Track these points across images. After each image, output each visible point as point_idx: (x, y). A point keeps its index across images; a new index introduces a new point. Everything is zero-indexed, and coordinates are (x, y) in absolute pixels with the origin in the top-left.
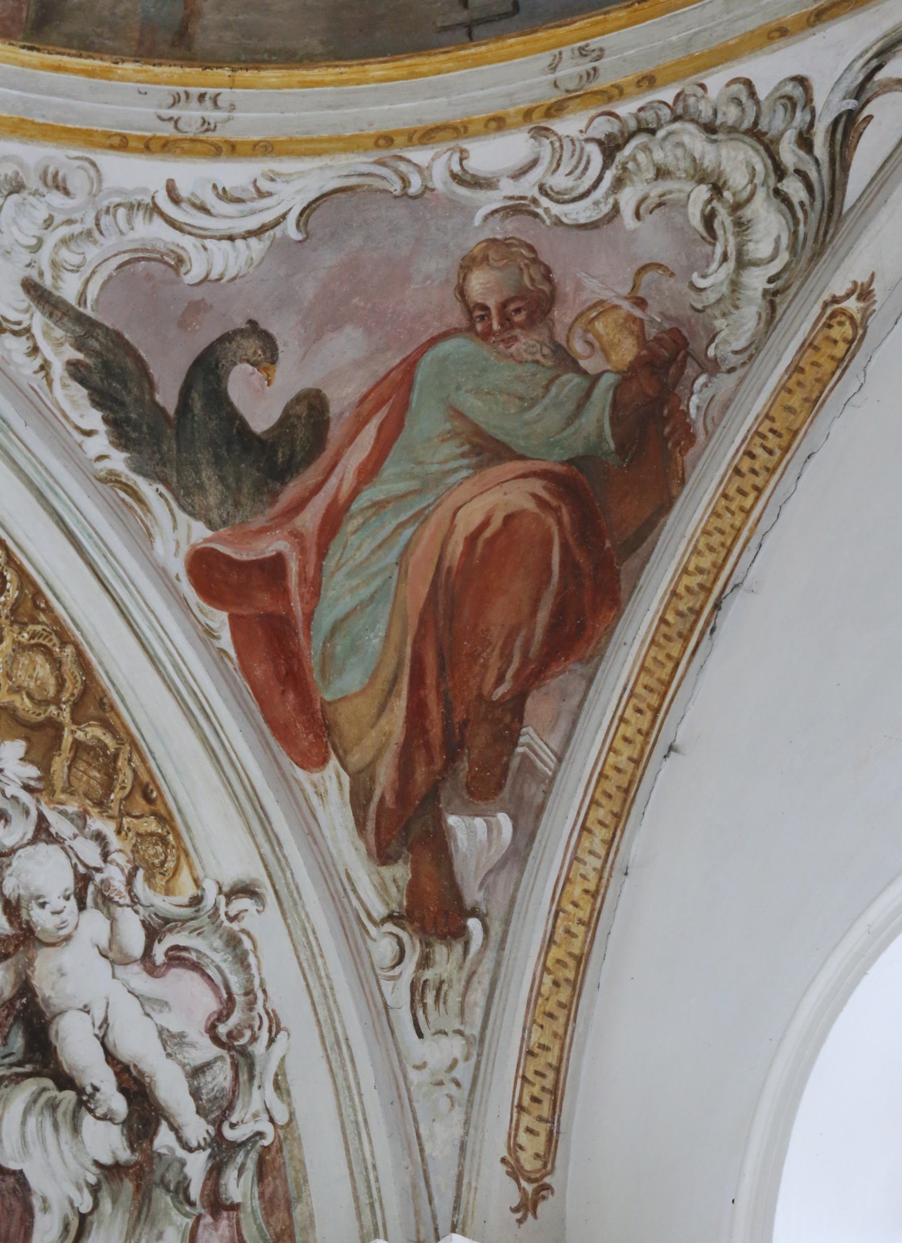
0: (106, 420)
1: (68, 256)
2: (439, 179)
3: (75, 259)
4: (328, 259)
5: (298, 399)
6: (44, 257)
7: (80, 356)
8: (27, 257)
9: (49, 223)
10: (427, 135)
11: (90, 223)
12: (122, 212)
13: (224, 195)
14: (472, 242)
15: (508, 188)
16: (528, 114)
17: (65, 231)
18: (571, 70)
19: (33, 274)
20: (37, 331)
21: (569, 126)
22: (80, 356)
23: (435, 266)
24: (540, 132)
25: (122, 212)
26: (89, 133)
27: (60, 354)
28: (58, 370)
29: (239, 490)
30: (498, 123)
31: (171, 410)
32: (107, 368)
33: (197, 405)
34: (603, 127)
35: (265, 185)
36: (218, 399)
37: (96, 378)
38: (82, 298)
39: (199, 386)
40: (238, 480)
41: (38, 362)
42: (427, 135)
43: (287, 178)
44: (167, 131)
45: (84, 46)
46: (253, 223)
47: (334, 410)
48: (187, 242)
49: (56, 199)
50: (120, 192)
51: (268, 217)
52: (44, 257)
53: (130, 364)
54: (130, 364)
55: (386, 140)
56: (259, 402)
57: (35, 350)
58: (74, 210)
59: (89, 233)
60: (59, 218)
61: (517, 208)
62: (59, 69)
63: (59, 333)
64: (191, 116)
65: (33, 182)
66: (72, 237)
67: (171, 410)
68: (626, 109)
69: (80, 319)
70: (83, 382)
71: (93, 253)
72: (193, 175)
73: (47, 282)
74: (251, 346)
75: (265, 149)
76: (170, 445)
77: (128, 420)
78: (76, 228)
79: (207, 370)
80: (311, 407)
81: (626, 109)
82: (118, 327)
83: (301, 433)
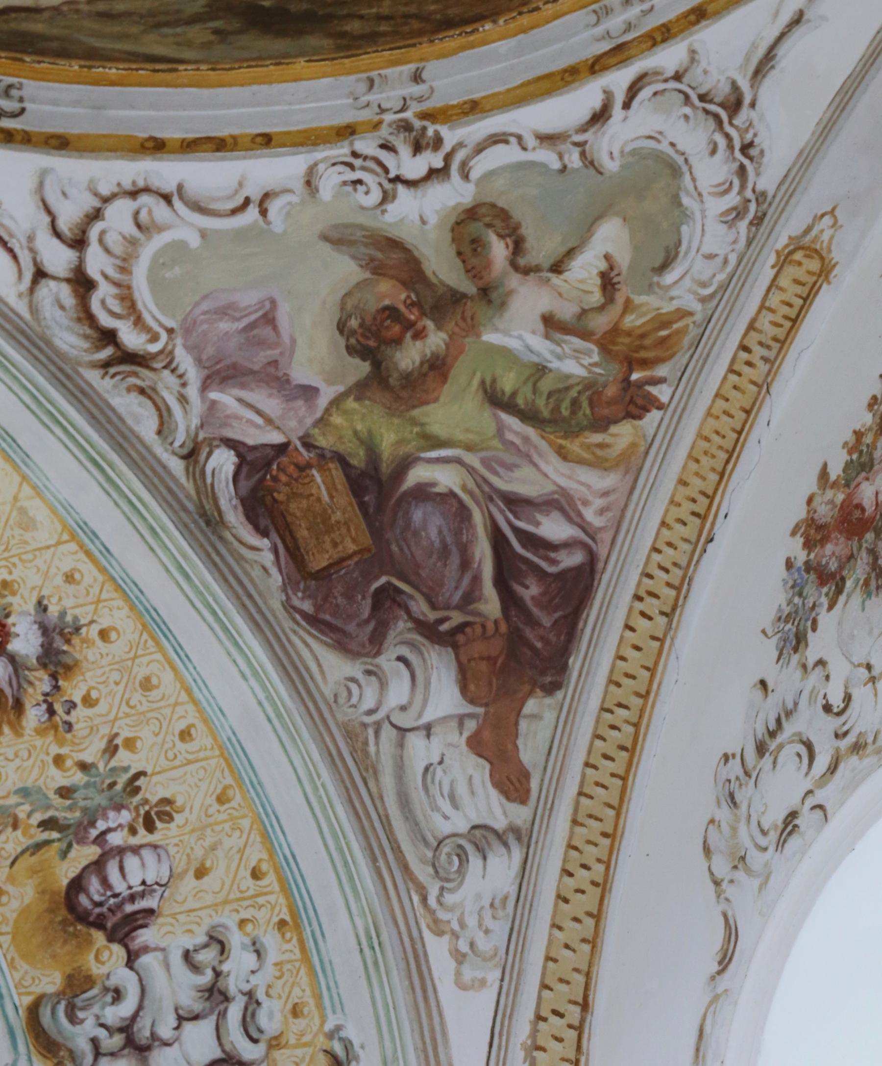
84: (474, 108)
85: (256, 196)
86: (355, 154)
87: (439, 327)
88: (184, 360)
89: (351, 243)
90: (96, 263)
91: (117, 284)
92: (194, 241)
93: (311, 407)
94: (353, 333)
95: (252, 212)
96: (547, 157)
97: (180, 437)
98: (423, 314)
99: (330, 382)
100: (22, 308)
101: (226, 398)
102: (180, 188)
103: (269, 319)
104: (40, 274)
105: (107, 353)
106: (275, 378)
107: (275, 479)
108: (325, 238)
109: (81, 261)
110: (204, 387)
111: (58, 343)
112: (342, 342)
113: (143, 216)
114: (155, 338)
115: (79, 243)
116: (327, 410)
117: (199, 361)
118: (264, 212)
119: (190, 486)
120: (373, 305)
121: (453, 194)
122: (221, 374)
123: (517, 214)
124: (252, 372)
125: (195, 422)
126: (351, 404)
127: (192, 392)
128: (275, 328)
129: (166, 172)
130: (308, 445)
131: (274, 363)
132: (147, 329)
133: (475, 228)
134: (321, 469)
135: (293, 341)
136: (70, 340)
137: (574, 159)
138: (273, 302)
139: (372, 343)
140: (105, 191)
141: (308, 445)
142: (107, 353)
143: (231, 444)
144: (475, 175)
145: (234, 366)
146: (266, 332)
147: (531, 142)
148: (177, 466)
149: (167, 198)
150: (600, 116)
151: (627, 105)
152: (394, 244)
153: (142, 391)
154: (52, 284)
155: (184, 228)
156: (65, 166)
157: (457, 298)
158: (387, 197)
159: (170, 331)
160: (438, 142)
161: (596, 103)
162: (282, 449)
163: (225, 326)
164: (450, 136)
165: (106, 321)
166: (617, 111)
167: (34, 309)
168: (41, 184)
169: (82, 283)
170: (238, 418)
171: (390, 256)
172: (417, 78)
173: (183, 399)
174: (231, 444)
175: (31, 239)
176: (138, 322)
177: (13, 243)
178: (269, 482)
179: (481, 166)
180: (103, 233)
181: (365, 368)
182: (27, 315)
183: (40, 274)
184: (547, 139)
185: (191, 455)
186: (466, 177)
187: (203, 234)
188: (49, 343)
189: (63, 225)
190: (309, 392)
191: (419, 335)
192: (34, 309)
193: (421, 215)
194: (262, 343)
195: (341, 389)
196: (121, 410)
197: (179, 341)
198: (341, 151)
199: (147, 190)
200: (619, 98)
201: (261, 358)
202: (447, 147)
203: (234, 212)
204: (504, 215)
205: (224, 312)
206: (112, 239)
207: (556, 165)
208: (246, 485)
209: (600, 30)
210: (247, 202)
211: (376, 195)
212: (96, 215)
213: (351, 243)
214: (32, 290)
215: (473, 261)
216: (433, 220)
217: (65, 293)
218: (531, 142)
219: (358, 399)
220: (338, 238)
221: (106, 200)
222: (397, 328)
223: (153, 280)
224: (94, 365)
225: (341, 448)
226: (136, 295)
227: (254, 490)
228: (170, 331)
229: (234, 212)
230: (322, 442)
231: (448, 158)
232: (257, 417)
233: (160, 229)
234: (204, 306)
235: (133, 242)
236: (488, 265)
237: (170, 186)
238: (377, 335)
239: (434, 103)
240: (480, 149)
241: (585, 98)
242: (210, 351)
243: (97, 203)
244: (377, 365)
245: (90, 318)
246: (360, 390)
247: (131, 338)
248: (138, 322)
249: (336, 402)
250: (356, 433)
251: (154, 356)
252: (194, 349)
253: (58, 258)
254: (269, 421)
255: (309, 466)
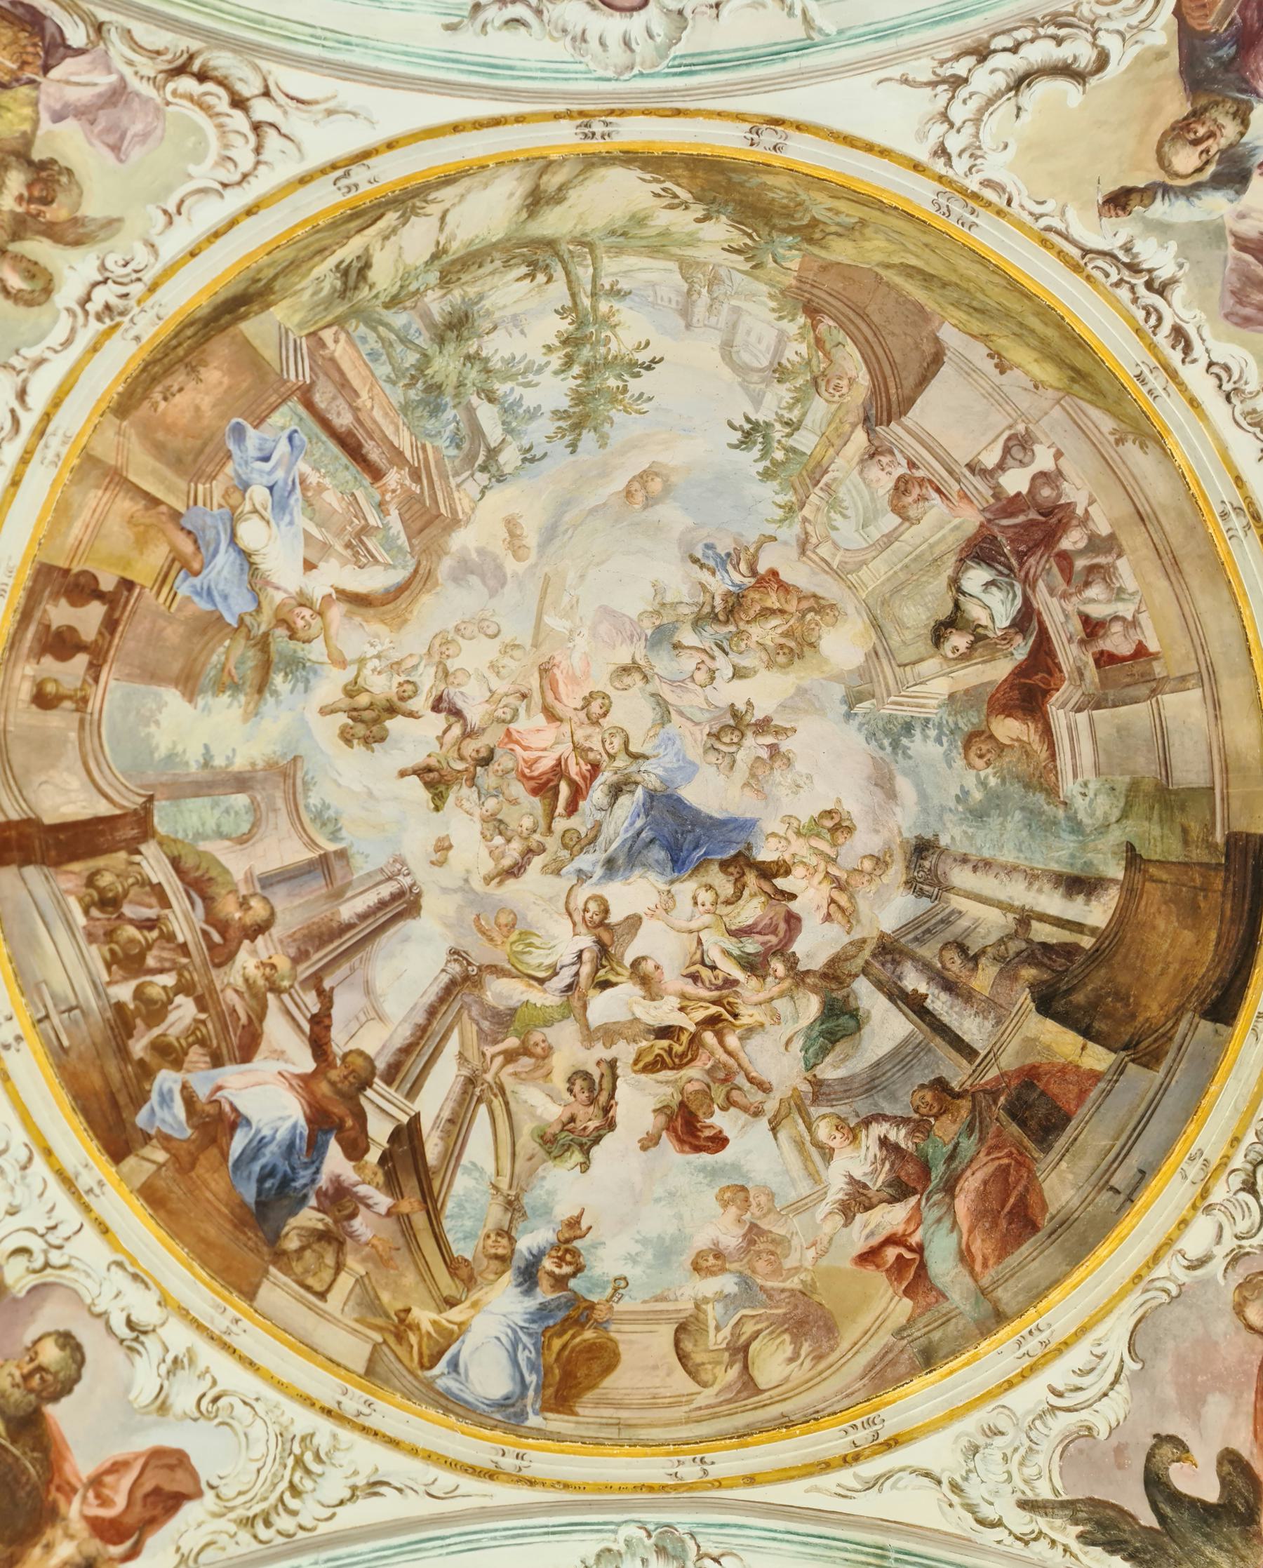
0: (1125, 1559)
1: (1030, 1471)
2: (1184, 1276)
3: (1035, 1471)
4: (1164, 1367)
5: (1220, 1464)
6: (1018, 1481)
7: (1080, 1528)
8: (1009, 1488)
9: (1006, 1459)
10: (1156, 1258)
11: (1027, 1443)
12: (1038, 1423)
13: (1083, 1373)
14: (1230, 1296)
15: (1220, 1252)
16: (1194, 1207)
17: (1017, 1457)
18: (1194, 1171)
19: (1019, 1495)
20: (1046, 1530)
21: (1219, 1193)
22: (1080, 1528)
23: (1224, 1325)
24: (1209, 1209)
25: (1038, 1423)
26: (989, 1392)
27: (1069, 1534)
28: (1075, 1546)
29: (1236, 1548)
30: (1184, 1223)
31: (1156, 1525)
32: (1100, 1524)
33: (1168, 1510)
34: (1237, 1181)
35: (1098, 1351)
36: (1177, 1499)
37: (1099, 1535)
38: (1056, 1492)
39: (1159, 1498)
40: (1230, 1541)
41: (1061, 1548)
42: (1156, 1258)
43: (1106, 1337)
44: (1027, 1362)
45: (954, 1353)
46: (1110, 1377)
47: (1245, 1454)
48: (1084, 1415)
49: (999, 1441)
50: (1028, 1412)
51: (1114, 1368)
52: (1018, 1481)
53: (1111, 1513)
54: (1111, 1513)
55: (1138, 1277)
56: (1200, 1482)
57: (1053, 1542)
58: (1013, 1441)
59: (1031, 1449)
60: (1009, 1452)
61: (1236, 1259)
62: (951, 1373)
63: (1058, 1522)
64: (1032, 1345)
65: (981, 1440)
66: (1024, 1458)
67: (1156, 1525)
68: (1238, 1161)
69: (1064, 1505)
70: (1094, 1544)
71: (1041, 1459)
72: (1058, 1373)
73: (1030, 1495)
74: (1167, 1450)
75: (1083, 1331)
76: (1173, 1548)
77: (1137, 1550)
78: (1022, 1451)
79: (1155, 1484)
80: (1231, 1462)
81: (1238, 1161)
82: (1088, 1495)
83: (1240, 1483)
84: (95, 348)
85: (176, 218)
86: (139, 280)
87: (12, 212)
88: (147, 90)
89: (102, 227)
90: (238, 120)
91: (218, 114)
92: (192, 169)
93: (49, 108)
94: (60, 173)
95: (172, 209)
96: (32, 353)
97: (114, 36)
98: (28, 213)
99: (49, 132)
100: (265, 65)
101: (105, 81)
102: (222, 196)
103: (115, 148)
104: (267, 94)
105: (196, 67)
106: (85, 113)
107: (35, 45)
108: (119, 220)
109: (249, 117)
110: (122, 79)
111: (229, 55)
112: (63, 163)
113: (230, 165)
114: (174, 93)
115: (257, 127)
116: (37, 113)
117: (138, 95)
118: (165, 212)
119: (85, 6)
120: (61, 198)
121: (67, 293)
122: (118, 95)
123: (21, 310)
124: (101, 108)
125: (112, 52)
126: (27, 127)
127: (128, 72)
128: (108, 146)
129: (237, 200)
130: (31, 82)
131: (92, 123)
132: (182, 96)
133: (39, 284)
134: (11, 71)
135: (91, 144)
136: (222, 61)
137: (16, 361)
138: (121, 161)
139: (44, 174)
140: (262, 168)
141: (31, 82)
142: (196, 67)
143: (80, 52)
144: (64, 314)
145: (115, 105)
146: (112, 139)
147: (48, 354)
148: (103, 15)
149: (225, 185)
150: (22, 395)
151: (12, 411)
152: (77, 243)
153: (158, 53)
154: (257, 92)
155: (205, 173)
156: (296, 169)
157: (16, 236)
158: (103, 267)
159: (168, 104)
160: (99, 318)
161: (29, 399)
162: (46, 69)
163: (138, 127)
164: (95, 326)
165: (210, 86)
166: (16, 405)
167: (257, 68)
168: (300, 150)
169: (239, 103)
170: (89, 72)
171: (73, 234)
172: (137, 338)
173: (130, 63)
174: (80, 52)
175: (285, 113)
176: (191, 98)
177: (293, 104)
178: (37, 40)
179: (65, 322)
180: (247, 141)
181: (37, 155)
182: (258, 61)
183: (267, 94)
184: (40, 362)
185: (99, 28)
186: (68, 310)
187: (190, 177)
188: (234, 51)
189: (271, 132)
190: (58, 117)
191: (20, 199)
192: (257, 68)
193: (74, 270)
194: (108, 130)
195: (40, 133)
196: (163, 32)
197: (159, 100)
198: (148, 277)
199: (239, 183)
200: (20, 412)
201: (102, 123)
202: (92, 319)
203: (182, 202)
204: (30, 303)
205: (145, 136)
206: (238, 141)
207: (23, 351)
208: (50, 29)
209: (60, 432)
210: (179, 213)
211: (110, 264)
212: (258, 150)
213: (102, 227)
214: (265, 80)
215: (24, 264)
216: (67, 272)
217: (245, 90)
218: (48, 354)
219: (24, 134)
220: (111, 225)
221: (258, 163)
222: (36, 193)
223: (198, 129)
224: (199, 52)
225: (10, 93)
226: (202, 114)
227: (42, 30)
228: (168, 104)
229: (182, 202)
230: (24, 91)
231: (86, 313)
232: (74, 80)
233: (217, 164)
234: (159, 132)
235: (227, 146)
236: (14, 268)
237: (228, 193)
238: (45, 181)
239: (117, 335)
240: (73, 330)
241: (39, 398)
242: (136, 104)
243: (262, 158)
244: (30, 163)
245: (221, 83)
246: (28, 140)
247: (187, 84)
248: (191, 98)
249: (36, 123)
250: (9, 110)
251: (166, 81)
252: (146, 101)
253: (262, 110)
254: (68, 82)
255: (21, 68)
